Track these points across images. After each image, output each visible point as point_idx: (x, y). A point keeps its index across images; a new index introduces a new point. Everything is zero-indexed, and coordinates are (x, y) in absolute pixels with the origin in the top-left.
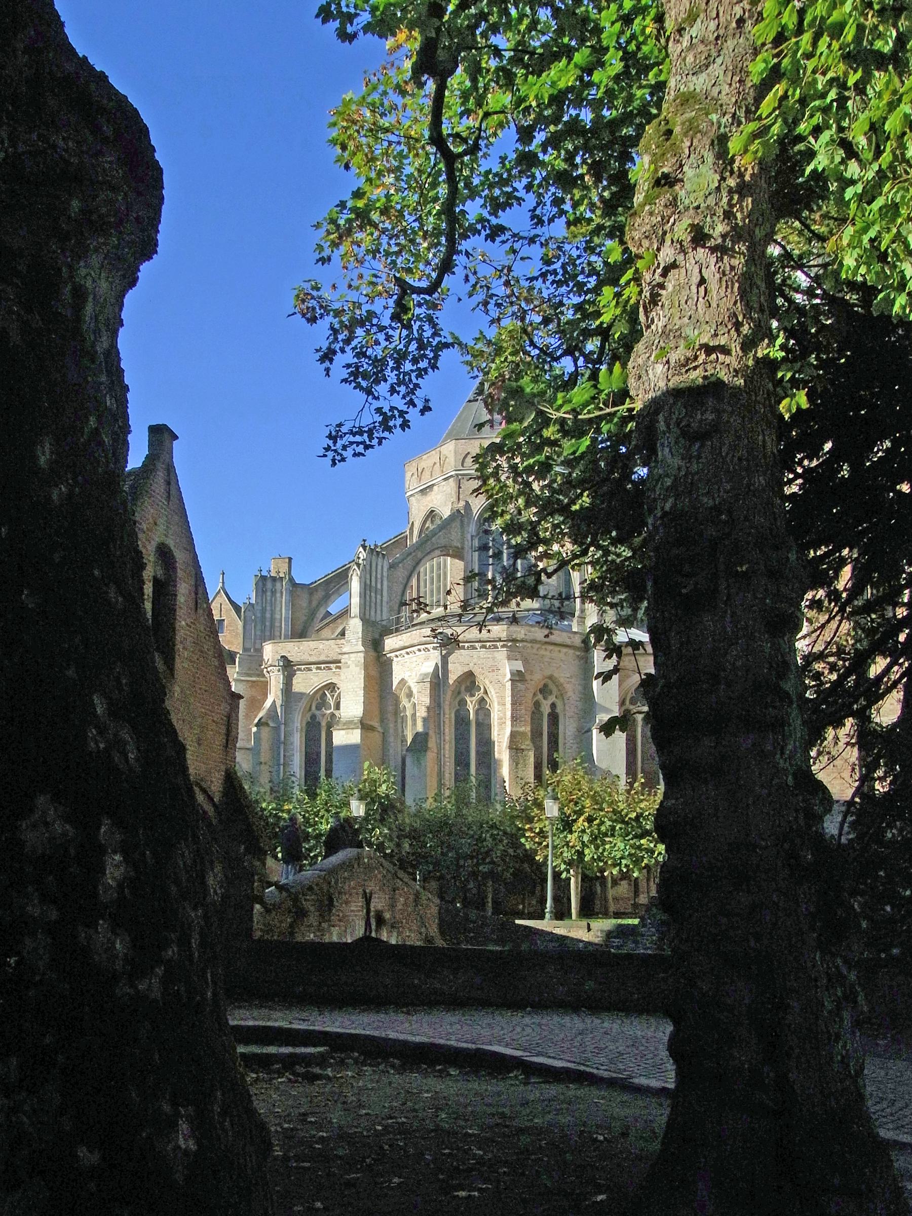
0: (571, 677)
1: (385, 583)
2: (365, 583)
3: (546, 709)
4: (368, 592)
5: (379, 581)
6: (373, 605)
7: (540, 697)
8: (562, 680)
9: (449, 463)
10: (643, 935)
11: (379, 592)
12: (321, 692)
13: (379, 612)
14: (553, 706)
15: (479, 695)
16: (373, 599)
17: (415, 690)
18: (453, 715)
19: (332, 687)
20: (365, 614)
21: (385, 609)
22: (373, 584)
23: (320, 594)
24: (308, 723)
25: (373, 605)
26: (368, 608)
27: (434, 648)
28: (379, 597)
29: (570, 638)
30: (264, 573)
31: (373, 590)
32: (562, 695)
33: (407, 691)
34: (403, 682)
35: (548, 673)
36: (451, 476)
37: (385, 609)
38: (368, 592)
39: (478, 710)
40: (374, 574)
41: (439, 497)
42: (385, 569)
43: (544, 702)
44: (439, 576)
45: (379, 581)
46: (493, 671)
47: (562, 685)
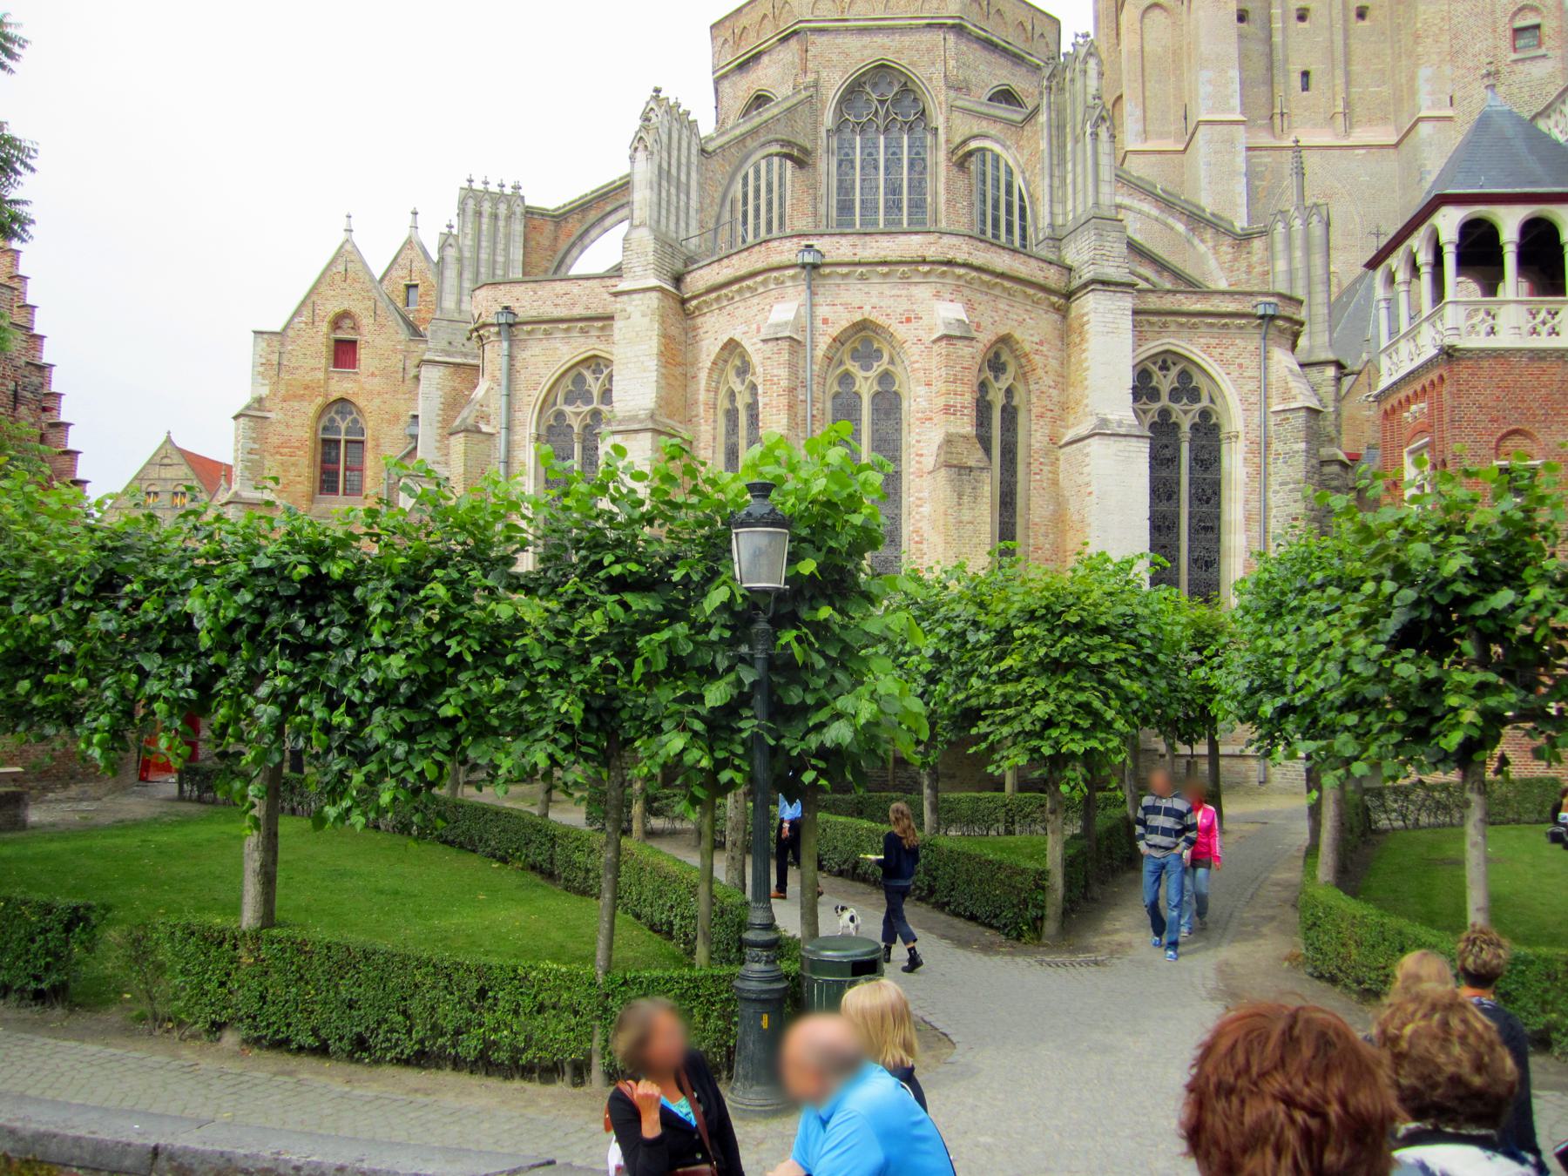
0: (1041, 343)
1: (694, 175)
2: (660, 166)
3: (997, 398)
4: (664, 183)
5: (684, 169)
6: (673, 210)
7: (989, 374)
8: (1027, 348)
9: (791, 12)
11: (683, 188)
12: (574, 373)
13: (682, 224)
14: (1009, 392)
15: (878, 368)
16: (674, 199)
17: (755, 359)
18: (829, 405)
19: (595, 363)
20: (659, 222)
21: (694, 224)
22: (674, 171)
23: (574, 226)
24: (550, 428)
25: (673, 210)
26: (664, 212)
27: (793, 278)
28: (683, 197)
29: (1041, 270)
30: (478, 186)
31: (674, 183)
32: (1024, 374)
33: (738, 363)
34: (732, 346)
35: (1003, 331)
36: (795, 33)
37: (694, 224)
38: (664, 183)
39: (877, 394)
40: (675, 153)
41: (770, 71)
42: (694, 151)
43: (997, 385)
44: (770, 203)
45: (684, 169)
46: (908, 320)
47: (1026, 355)
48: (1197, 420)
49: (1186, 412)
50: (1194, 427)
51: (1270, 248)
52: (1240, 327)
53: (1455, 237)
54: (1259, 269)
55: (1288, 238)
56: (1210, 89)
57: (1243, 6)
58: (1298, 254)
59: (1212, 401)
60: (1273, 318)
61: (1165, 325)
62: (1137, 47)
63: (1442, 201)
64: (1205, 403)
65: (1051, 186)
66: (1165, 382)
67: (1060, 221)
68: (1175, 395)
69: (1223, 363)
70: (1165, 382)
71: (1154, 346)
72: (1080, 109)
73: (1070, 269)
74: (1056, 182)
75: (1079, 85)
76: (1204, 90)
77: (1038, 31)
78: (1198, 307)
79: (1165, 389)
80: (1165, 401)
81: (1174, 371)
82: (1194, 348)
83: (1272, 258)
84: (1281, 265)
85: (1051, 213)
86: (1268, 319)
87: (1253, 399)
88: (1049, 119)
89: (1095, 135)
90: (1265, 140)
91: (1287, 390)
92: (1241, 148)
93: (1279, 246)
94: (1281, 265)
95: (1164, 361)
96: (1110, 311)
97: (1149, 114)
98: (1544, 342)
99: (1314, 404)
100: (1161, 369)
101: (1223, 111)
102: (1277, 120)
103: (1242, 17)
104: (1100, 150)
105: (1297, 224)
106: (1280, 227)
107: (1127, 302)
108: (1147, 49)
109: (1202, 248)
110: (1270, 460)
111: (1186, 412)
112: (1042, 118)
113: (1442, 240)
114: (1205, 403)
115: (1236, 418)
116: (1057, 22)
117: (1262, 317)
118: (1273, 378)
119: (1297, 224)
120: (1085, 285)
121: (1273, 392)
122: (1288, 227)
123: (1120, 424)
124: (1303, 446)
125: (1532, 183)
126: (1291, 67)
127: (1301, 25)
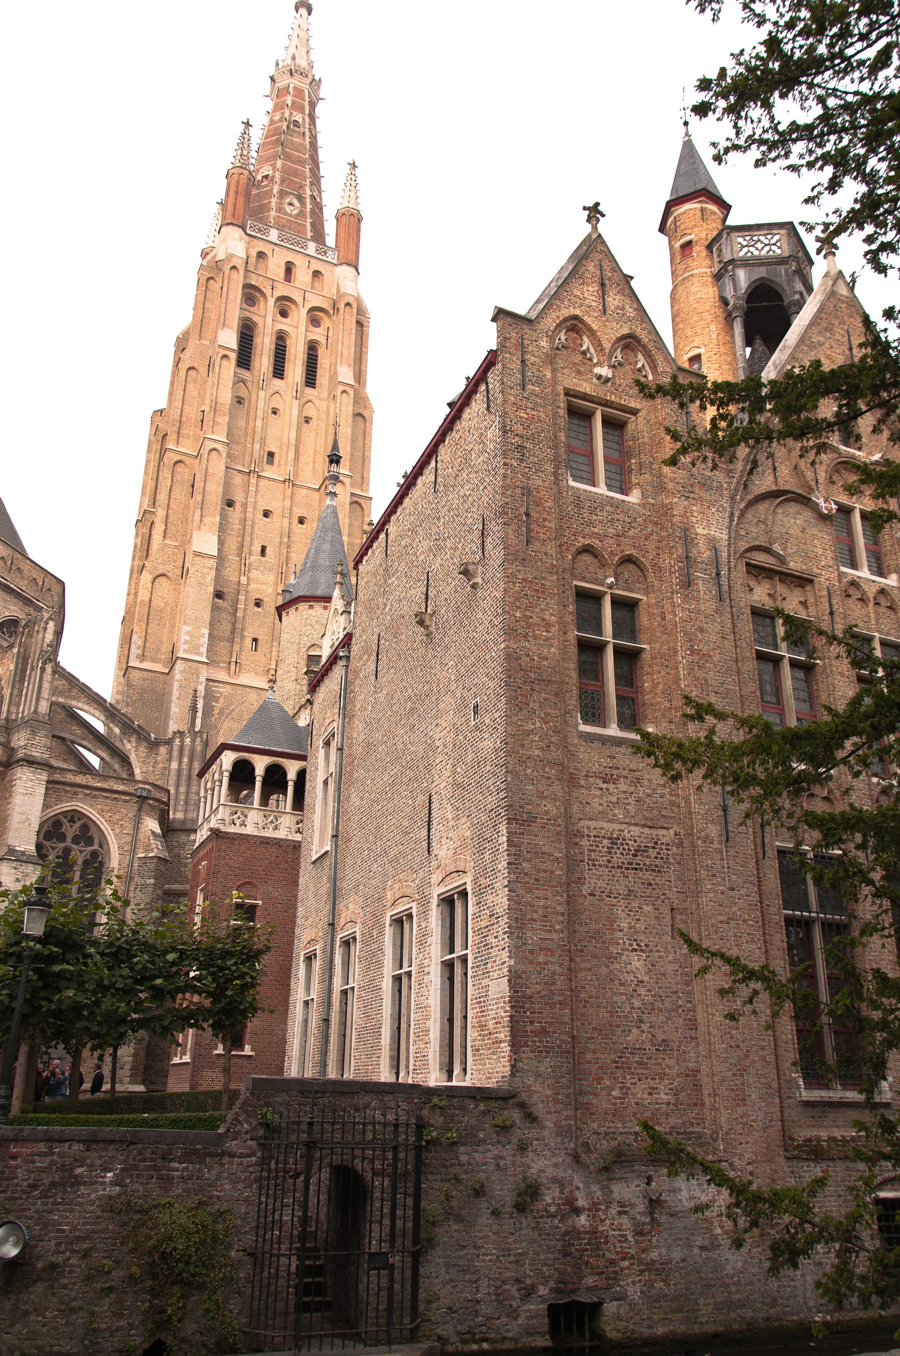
10: (232, 1155)
48: (88, 857)
49: (81, 852)
50: (86, 863)
51: (170, 753)
52: (126, 801)
53: (230, 768)
54: (161, 765)
55: (182, 748)
56: (188, 638)
57: (219, 588)
58: (186, 760)
59: (101, 846)
60: (146, 798)
61: (75, 793)
62: (147, 599)
63: (225, 747)
64: (96, 847)
65: (11, 694)
66: (71, 830)
67: (13, 717)
68: (76, 840)
69: (109, 822)
70: (71, 830)
71: (66, 806)
72: (38, 651)
73: (13, 749)
74: (16, 692)
75: (40, 636)
76: (185, 637)
77: (47, 586)
78: (99, 785)
79: (70, 836)
80: (69, 842)
81: (78, 824)
82: (92, 812)
83: (170, 760)
84: (174, 765)
85: (8, 711)
86: (143, 799)
87: (127, 848)
88: (19, 652)
89: (43, 669)
90: (222, 676)
91: (149, 845)
92: (202, 679)
93: (175, 753)
94: (174, 765)
95: (72, 817)
96: (31, 780)
97: (148, 645)
98: (269, 833)
99: (165, 854)
100: (69, 821)
101: (195, 654)
102: (233, 666)
103: (219, 595)
104: (45, 678)
105: (188, 741)
106: (177, 741)
107: (44, 776)
108: (154, 602)
109: (128, 746)
110: (132, 888)
111: (81, 852)
112: (15, 650)
113: (224, 768)
114: (96, 847)
115: (115, 861)
116: (62, 584)
117: (139, 797)
118: (141, 836)
119: (188, 741)
120: (18, 761)
121: (140, 845)
122: (182, 741)
123: (23, 853)
124: (152, 881)
125: (264, 744)
126: (246, 634)
127: (256, 609)
